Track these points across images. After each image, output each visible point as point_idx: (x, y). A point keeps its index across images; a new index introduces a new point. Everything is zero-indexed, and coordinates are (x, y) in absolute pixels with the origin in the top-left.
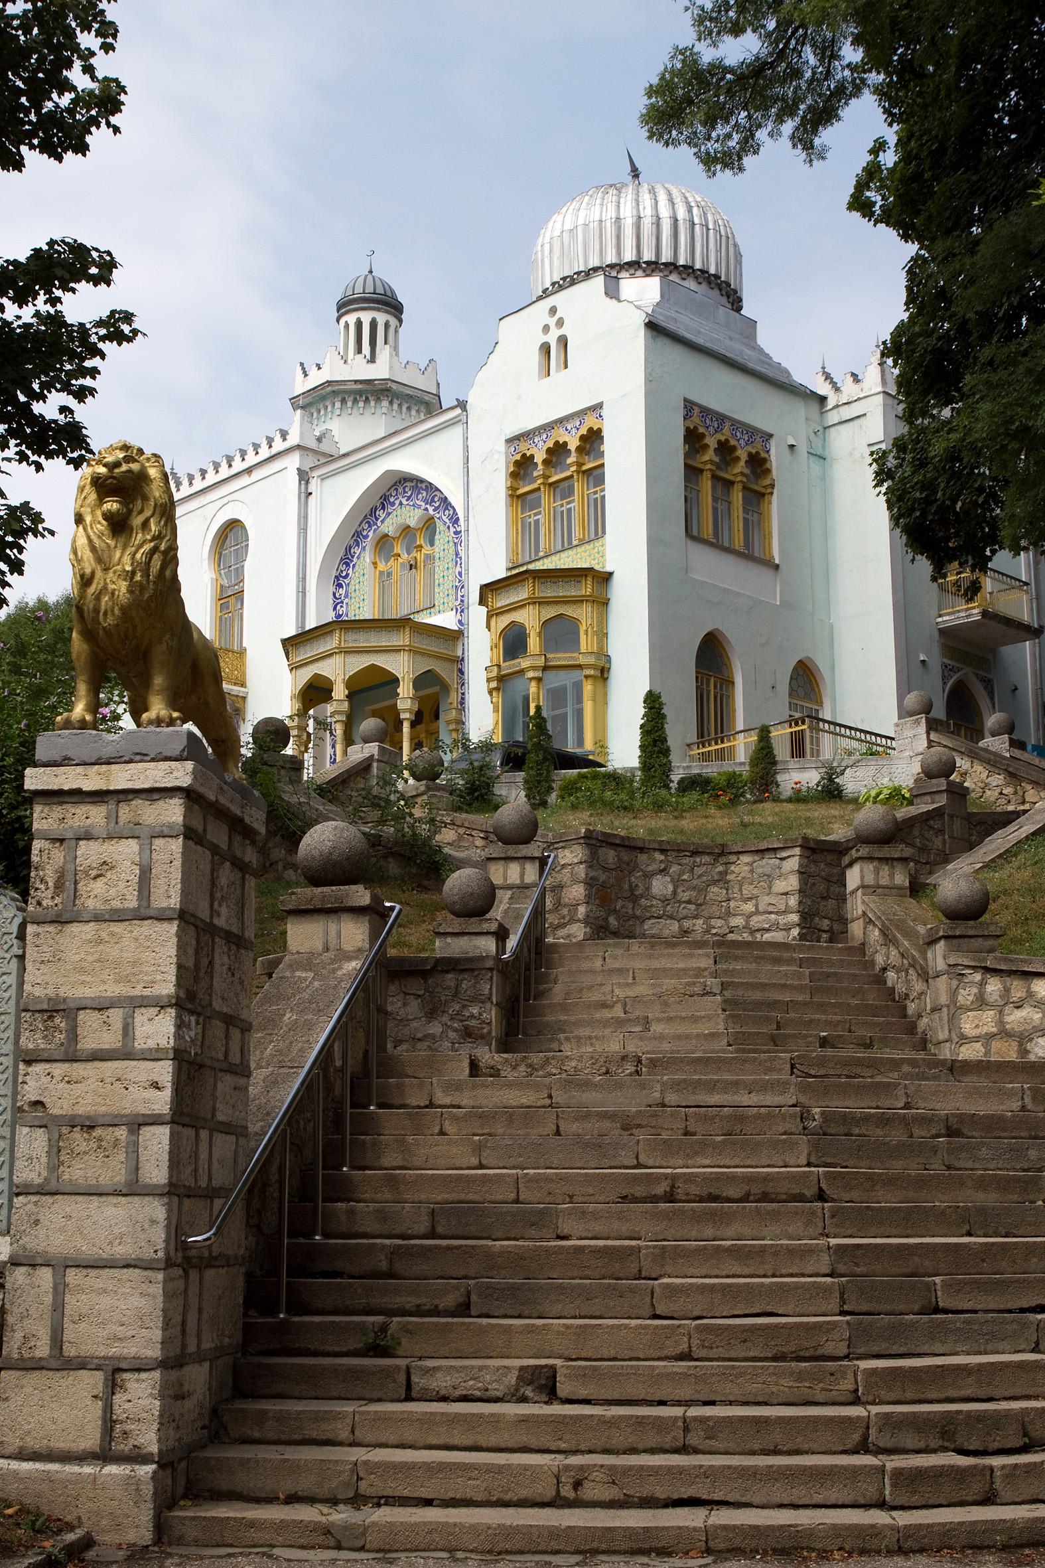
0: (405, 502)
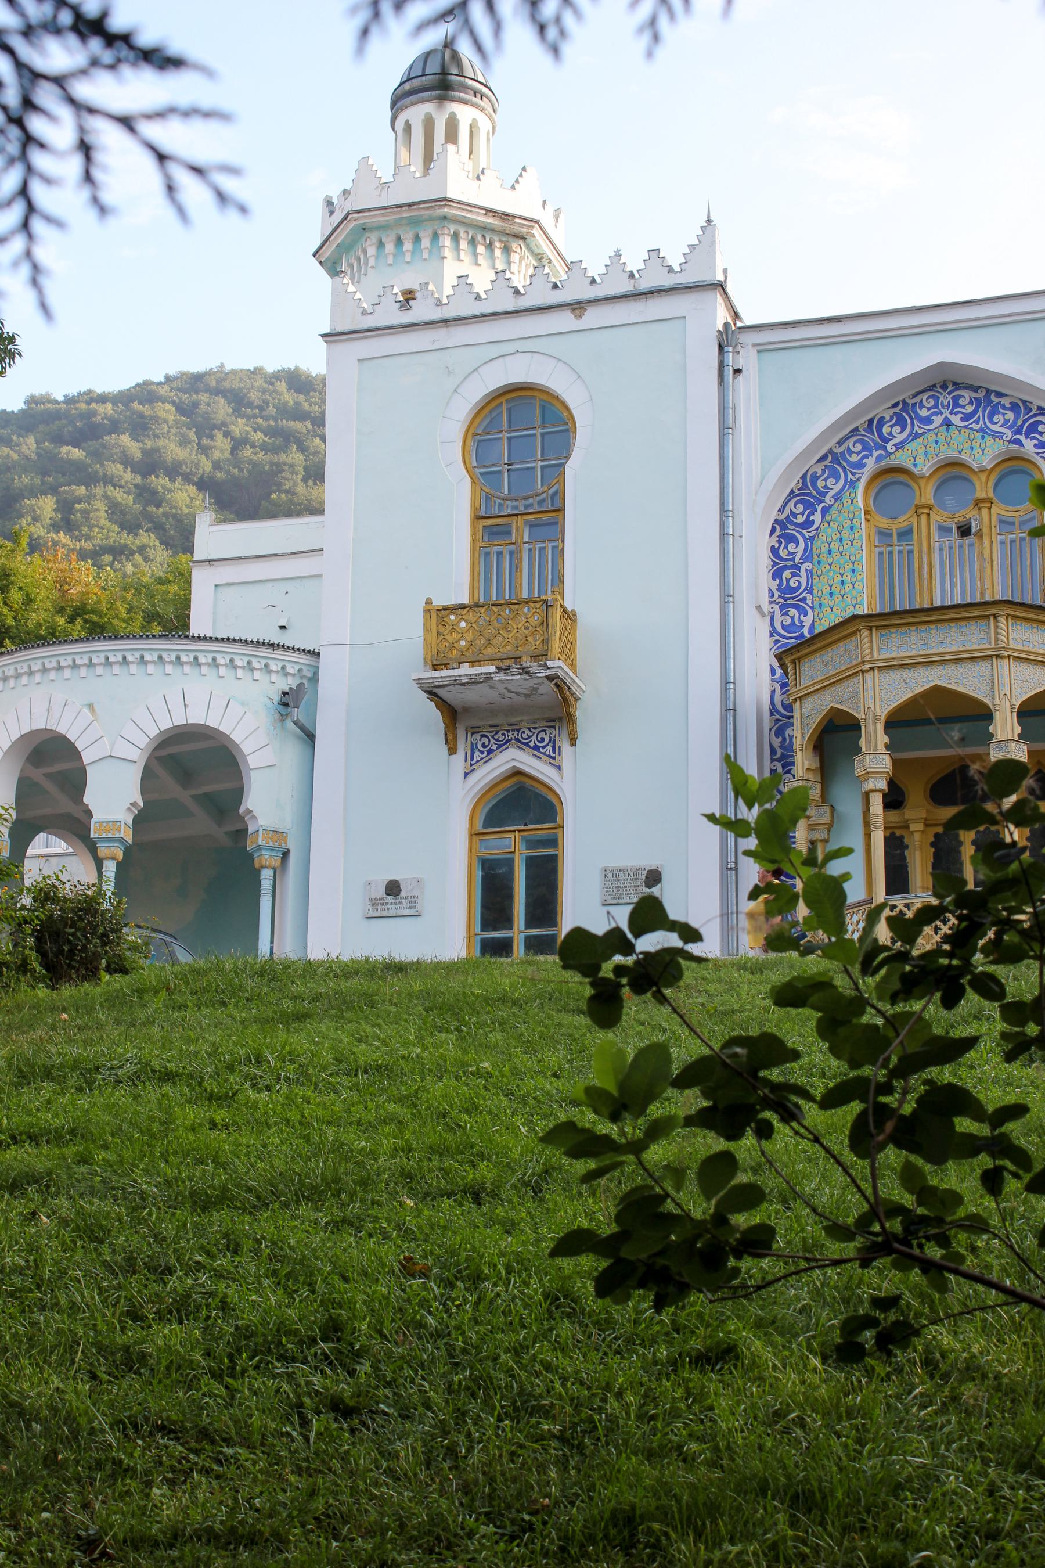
0: (956, 420)
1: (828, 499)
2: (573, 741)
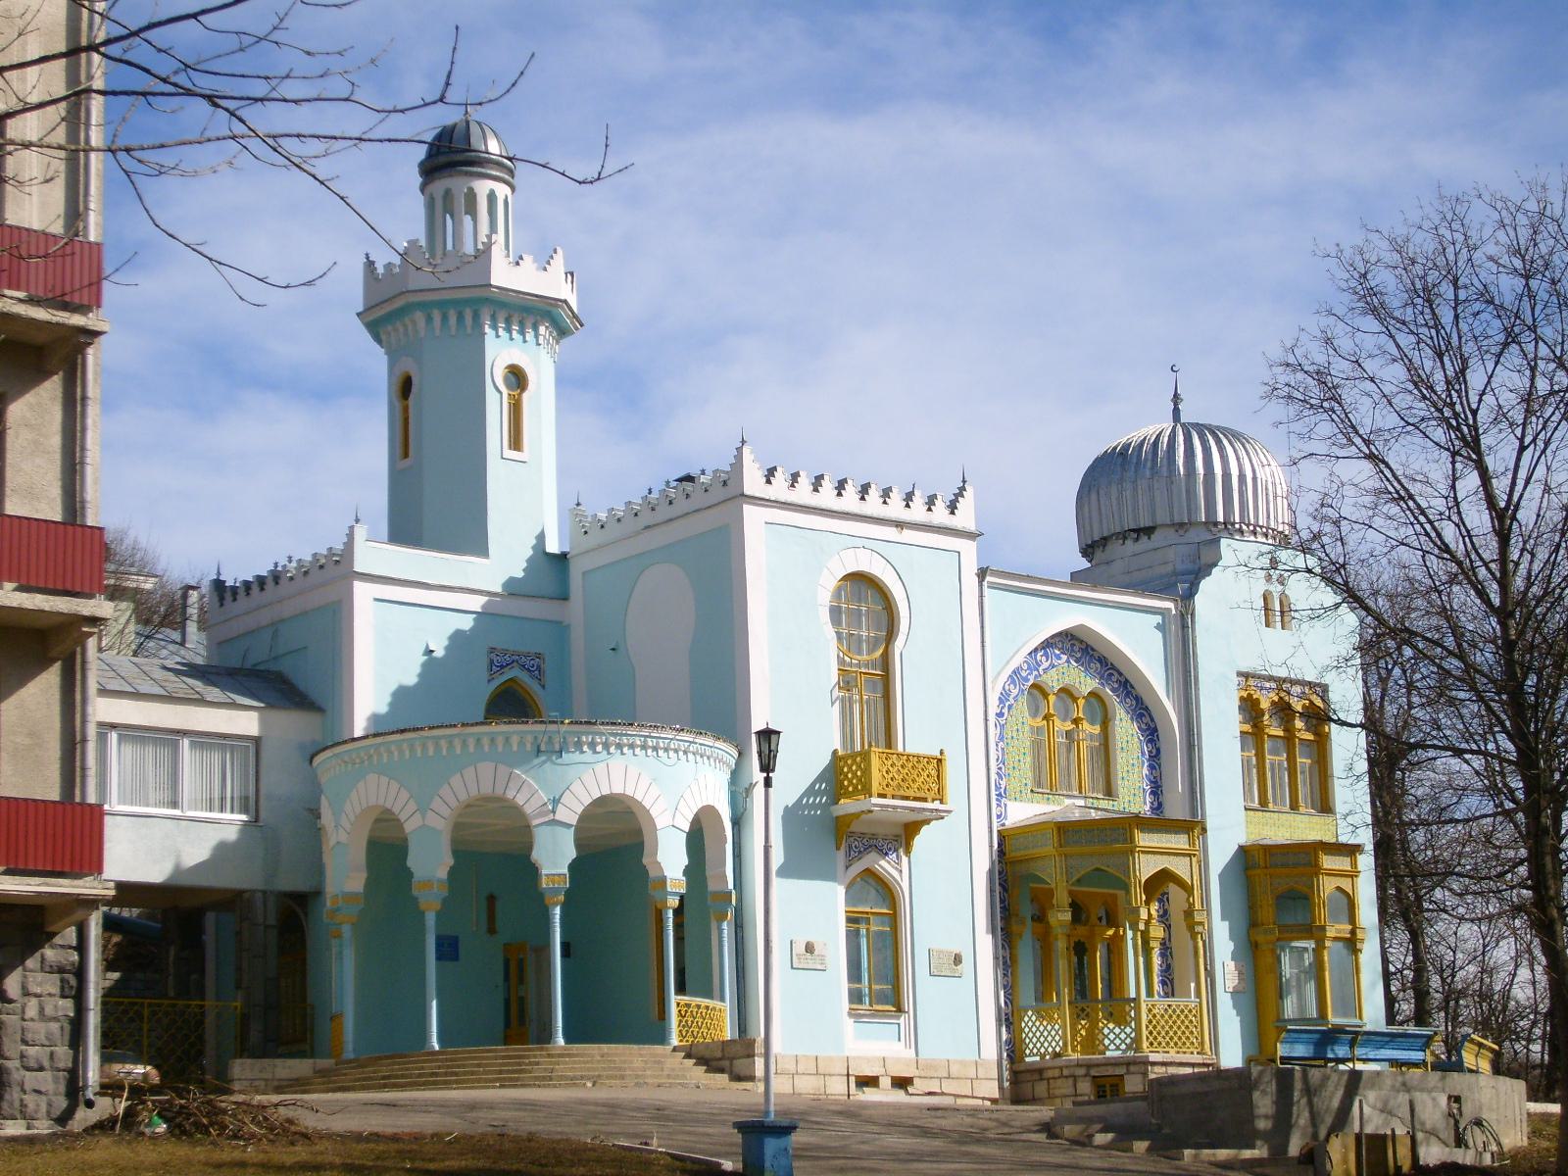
1: (1011, 698)
2: (908, 852)
